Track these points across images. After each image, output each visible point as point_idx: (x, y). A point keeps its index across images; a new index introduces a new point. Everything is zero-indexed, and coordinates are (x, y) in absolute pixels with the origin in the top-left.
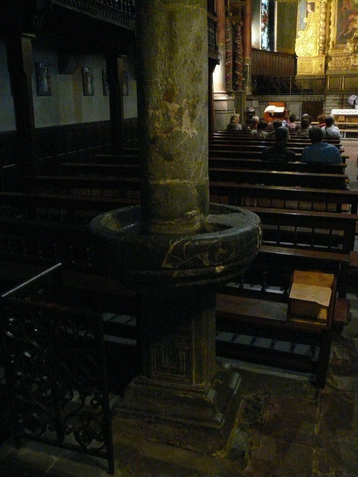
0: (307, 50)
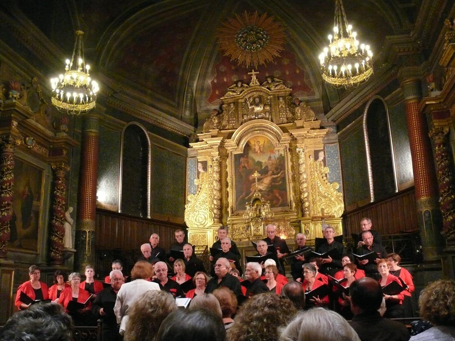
0: (200, 219)
